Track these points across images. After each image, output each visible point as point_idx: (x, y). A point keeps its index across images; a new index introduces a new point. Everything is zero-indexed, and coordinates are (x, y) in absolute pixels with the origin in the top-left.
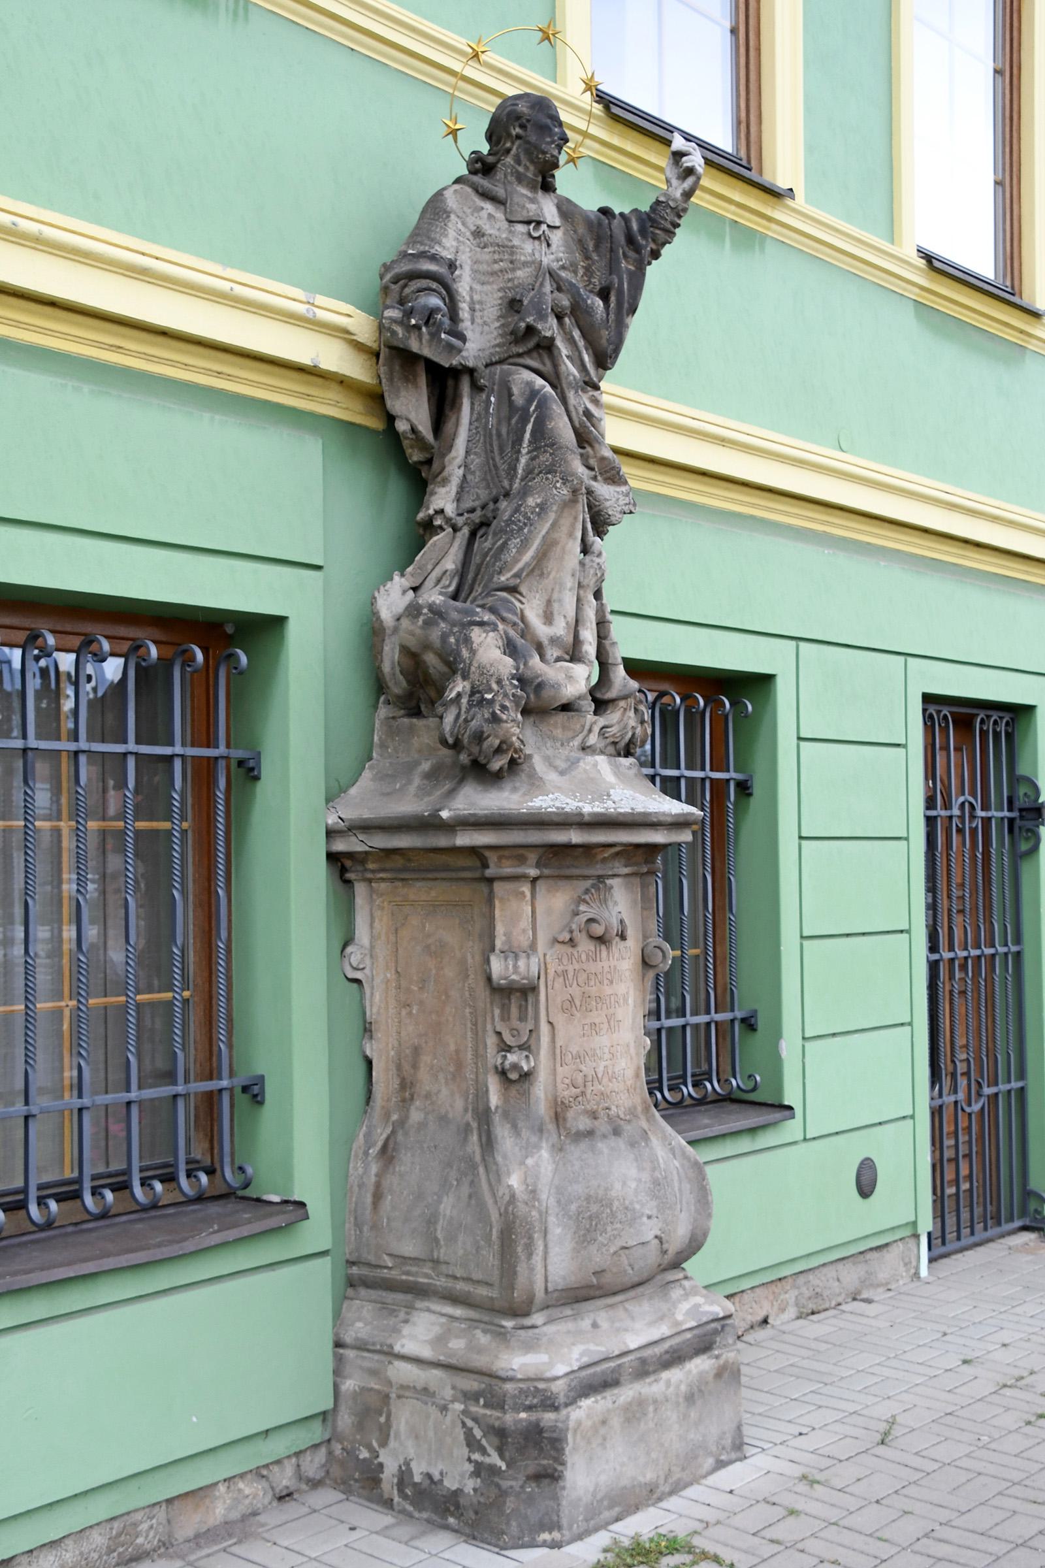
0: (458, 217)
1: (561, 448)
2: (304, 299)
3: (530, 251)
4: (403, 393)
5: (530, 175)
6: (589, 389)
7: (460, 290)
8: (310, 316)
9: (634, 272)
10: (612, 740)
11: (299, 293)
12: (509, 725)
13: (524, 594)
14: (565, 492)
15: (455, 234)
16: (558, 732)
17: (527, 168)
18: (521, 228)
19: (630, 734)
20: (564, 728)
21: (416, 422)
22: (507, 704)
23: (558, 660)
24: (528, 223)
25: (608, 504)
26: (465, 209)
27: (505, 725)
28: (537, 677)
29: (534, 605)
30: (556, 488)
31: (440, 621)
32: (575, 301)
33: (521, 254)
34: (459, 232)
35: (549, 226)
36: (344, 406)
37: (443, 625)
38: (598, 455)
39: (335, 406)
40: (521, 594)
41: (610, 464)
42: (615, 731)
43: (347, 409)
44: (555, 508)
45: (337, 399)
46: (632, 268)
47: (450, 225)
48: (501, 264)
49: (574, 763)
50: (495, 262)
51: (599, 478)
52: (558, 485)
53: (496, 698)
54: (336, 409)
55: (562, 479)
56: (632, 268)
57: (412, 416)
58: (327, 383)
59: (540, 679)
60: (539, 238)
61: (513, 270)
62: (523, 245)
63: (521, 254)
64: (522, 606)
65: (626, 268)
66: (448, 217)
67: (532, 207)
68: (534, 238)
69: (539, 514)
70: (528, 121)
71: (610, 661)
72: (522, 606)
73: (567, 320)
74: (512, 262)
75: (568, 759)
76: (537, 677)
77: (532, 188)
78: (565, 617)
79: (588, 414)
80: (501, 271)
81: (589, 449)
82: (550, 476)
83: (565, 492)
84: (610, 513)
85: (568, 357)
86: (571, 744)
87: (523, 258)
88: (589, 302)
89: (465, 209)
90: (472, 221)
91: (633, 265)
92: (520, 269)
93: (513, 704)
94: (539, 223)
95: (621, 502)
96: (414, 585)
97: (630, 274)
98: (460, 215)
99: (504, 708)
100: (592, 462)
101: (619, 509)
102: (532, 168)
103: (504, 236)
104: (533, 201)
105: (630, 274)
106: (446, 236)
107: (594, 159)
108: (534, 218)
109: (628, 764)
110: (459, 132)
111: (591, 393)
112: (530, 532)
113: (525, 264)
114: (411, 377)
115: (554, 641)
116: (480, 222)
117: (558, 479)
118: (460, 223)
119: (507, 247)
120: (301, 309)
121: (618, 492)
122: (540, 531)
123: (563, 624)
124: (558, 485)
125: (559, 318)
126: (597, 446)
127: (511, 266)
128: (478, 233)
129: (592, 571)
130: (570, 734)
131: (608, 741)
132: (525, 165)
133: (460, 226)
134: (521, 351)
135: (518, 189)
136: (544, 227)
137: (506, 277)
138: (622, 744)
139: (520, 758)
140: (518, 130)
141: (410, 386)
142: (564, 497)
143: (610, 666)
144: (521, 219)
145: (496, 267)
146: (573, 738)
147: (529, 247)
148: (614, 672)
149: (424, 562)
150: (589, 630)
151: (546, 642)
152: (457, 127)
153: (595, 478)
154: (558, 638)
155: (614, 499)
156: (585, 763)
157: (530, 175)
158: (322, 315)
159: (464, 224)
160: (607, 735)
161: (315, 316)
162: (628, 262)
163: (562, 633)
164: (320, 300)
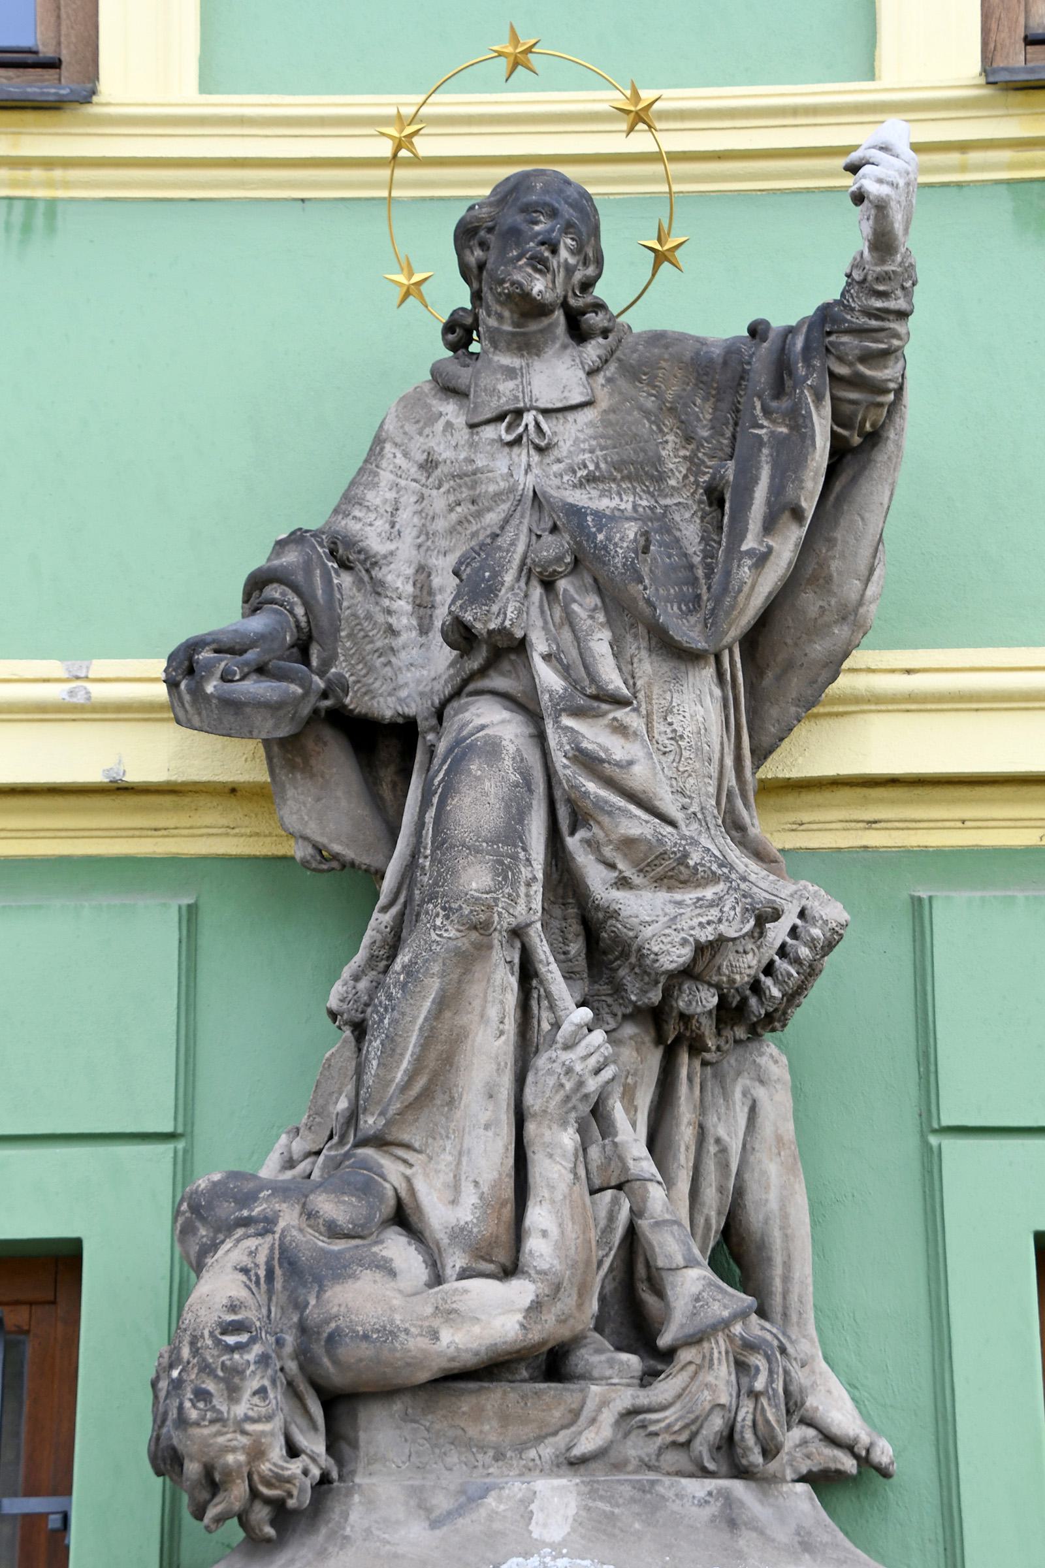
0: (396, 444)
1: (452, 846)
2: (64, 674)
3: (506, 470)
4: (291, 792)
5: (508, 328)
6: (605, 707)
7: (389, 578)
8: (80, 699)
9: (787, 437)
10: (669, 1439)
11: (53, 667)
12: (206, 1431)
13: (417, 1145)
14: (452, 933)
15: (392, 477)
16: (489, 1431)
17: (500, 317)
18: (489, 432)
19: (717, 1423)
20: (505, 1419)
21: (322, 840)
22: (210, 1386)
23: (464, 1275)
24: (500, 418)
25: (648, 932)
26: (408, 428)
27: (196, 1431)
28: (327, 1322)
29: (442, 1166)
30: (435, 928)
31: (198, 1224)
32: (576, 543)
33: (490, 480)
34: (398, 472)
35: (546, 412)
36: (248, 831)
37: (203, 1232)
38: (613, 837)
39: (227, 834)
40: (408, 1147)
41: (651, 847)
42: (672, 1419)
43: (257, 834)
44: (436, 968)
45: (224, 821)
46: (784, 430)
47: (384, 464)
48: (459, 509)
49: (470, 1498)
50: (451, 510)
51: (637, 880)
52: (438, 922)
53: (185, 1376)
54: (235, 840)
55: (444, 909)
56: (784, 430)
57: (312, 830)
58: (186, 800)
59: (333, 1325)
60: (517, 441)
61: (478, 515)
62: (492, 464)
63: (490, 480)
64: (408, 1172)
65: (772, 433)
66: (382, 449)
67: (507, 387)
68: (510, 444)
69: (404, 986)
70: (490, 230)
71: (660, 1264)
72: (408, 1172)
73: (562, 584)
74: (473, 502)
75: (462, 1492)
76: (327, 1322)
77: (520, 349)
78: (476, 1183)
79: (588, 761)
80: (460, 523)
81: (596, 829)
82: (431, 906)
83: (452, 933)
84: (656, 949)
85: (547, 658)
86: (532, 1453)
87: (492, 488)
88: (600, 537)
89: (408, 428)
90: (418, 448)
91: (783, 424)
92: (489, 510)
93: (222, 1386)
94: (519, 413)
95: (684, 923)
96: (317, 1148)
97: (779, 443)
98: (398, 440)
99: (202, 1395)
100: (608, 852)
101: (677, 937)
102: (507, 314)
103: (462, 456)
104: (511, 373)
105: (779, 443)
106: (375, 485)
107: (1008, 182)
108: (506, 408)
109: (701, 1494)
110: (423, 288)
111: (611, 716)
112: (394, 1022)
113: (497, 497)
114: (299, 760)
115: (458, 1234)
116: (432, 443)
117: (438, 909)
118: (399, 455)
119: (466, 475)
120: (55, 692)
121: (680, 904)
122: (415, 1018)
123: (474, 1199)
124: (438, 922)
125: (548, 585)
126: (605, 820)
127: (473, 508)
128: (429, 464)
129: (551, 1081)
130: (528, 1431)
131: (659, 1441)
132: (496, 313)
133: (400, 460)
134: (476, 665)
135: (496, 358)
136: (529, 418)
137: (468, 532)
138: (701, 1447)
139: (290, 1495)
140: (478, 253)
141: (299, 776)
142: (452, 944)
143: (664, 1274)
144: (488, 416)
145: (454, 517)
146: (540, 1439)
147: (501, 464)
148: (674, 1287)
149: (321, 1102)
150: (546, 1205)
151: (445, 1241)
152: (416, 278)
153: (623, 883)
154: (462, 1229)
155: (663, 919)
156: (500, 1500)
157: (508, 328)
158: (101, 692)
159: (406, 455)
160: (652, 1428)
161: (89, 698)
162: (773, 422)
163: (469, 1218)
164: (100, 667)
